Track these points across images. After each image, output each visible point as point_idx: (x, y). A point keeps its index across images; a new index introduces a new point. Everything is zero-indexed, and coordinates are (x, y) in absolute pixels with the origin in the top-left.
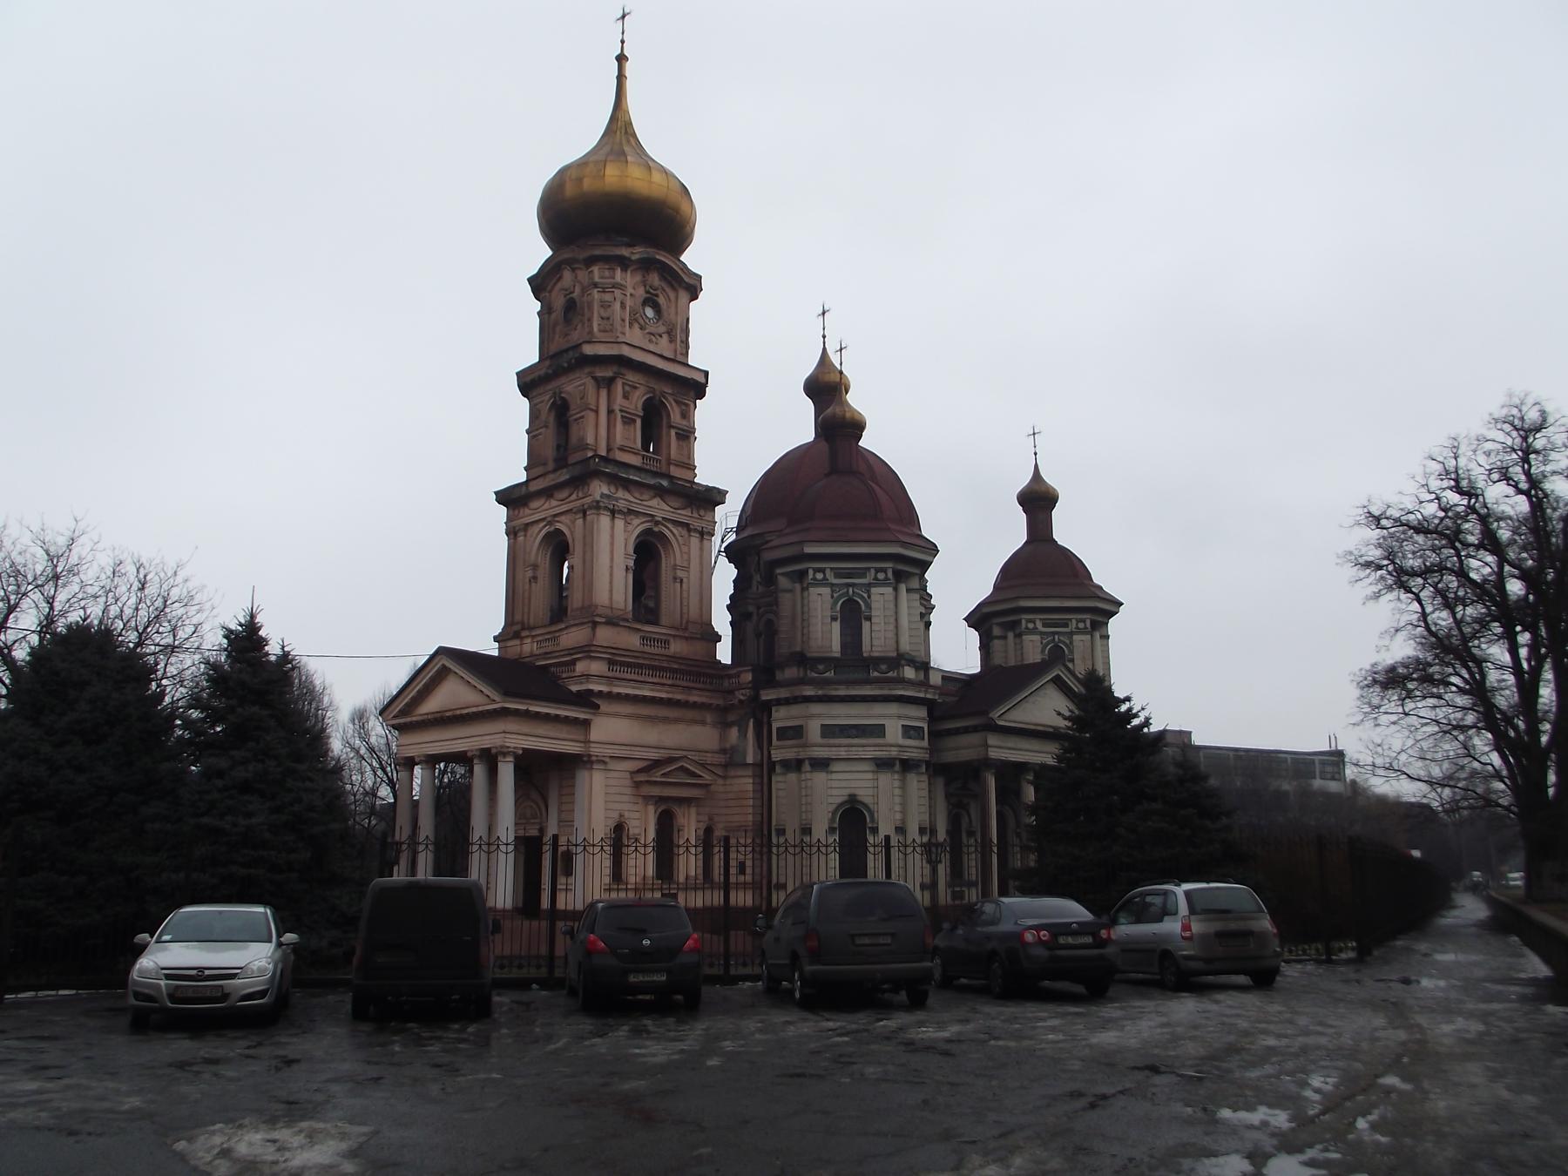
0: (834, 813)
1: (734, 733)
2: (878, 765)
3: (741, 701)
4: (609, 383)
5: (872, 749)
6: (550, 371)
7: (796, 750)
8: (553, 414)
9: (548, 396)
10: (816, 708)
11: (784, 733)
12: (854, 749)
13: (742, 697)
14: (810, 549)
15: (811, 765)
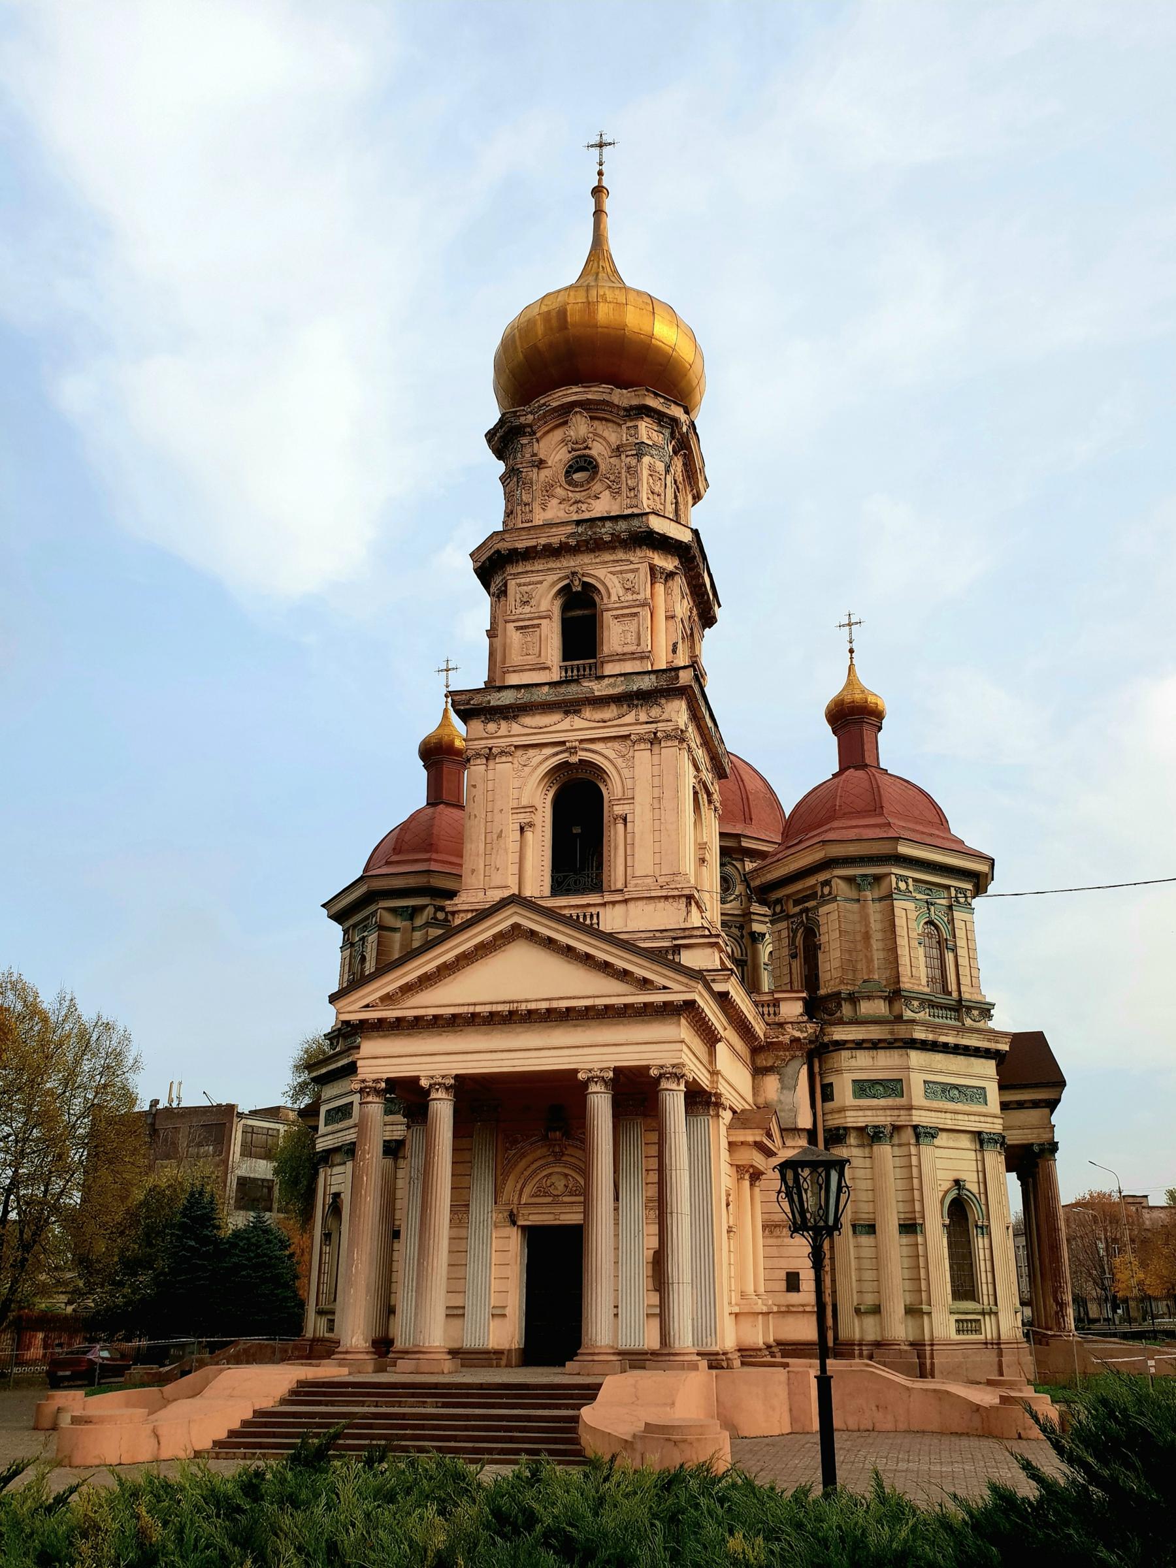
0: (942, 1202)
1: (771, 1084)
2: (981, 1142)
3: (795, 1040)
4: (670, 575)
5: (977, 1118)
6: (572, 542)
7: (896, 1112)
8: (558, 603)
9: (556, 577)
10: (916, 1058)
11: (863, 1088)
12: (960, 1117)
13: (798, 1034)
14: (904, 849)
15: (917, 1136)
